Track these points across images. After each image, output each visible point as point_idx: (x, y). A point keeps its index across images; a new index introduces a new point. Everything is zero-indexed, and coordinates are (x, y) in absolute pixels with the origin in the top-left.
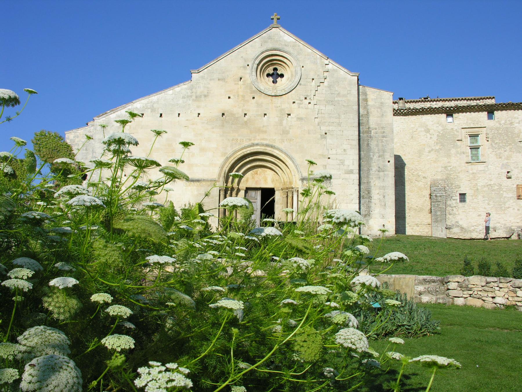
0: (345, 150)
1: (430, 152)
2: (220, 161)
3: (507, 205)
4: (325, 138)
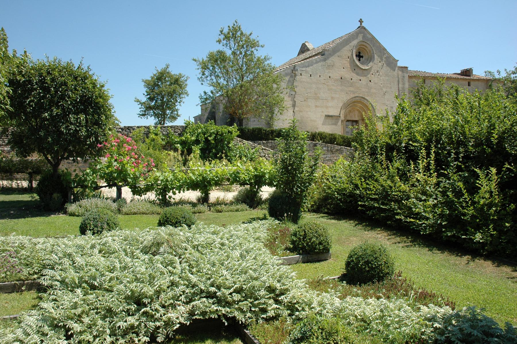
2: (341, 105)
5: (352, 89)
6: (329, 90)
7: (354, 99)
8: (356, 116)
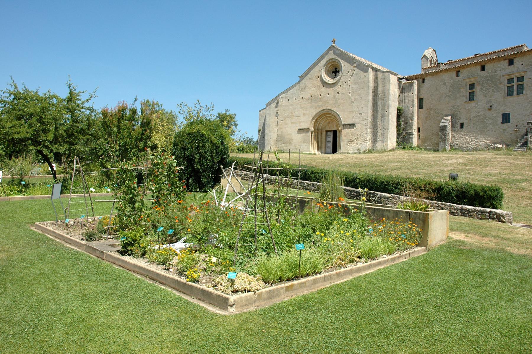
1: (445, 97)
2: (311, 118)
3: (488, 129)
5: (320, 103)
6: (302, 108)
7: (326, 111)
8: (335, 126)
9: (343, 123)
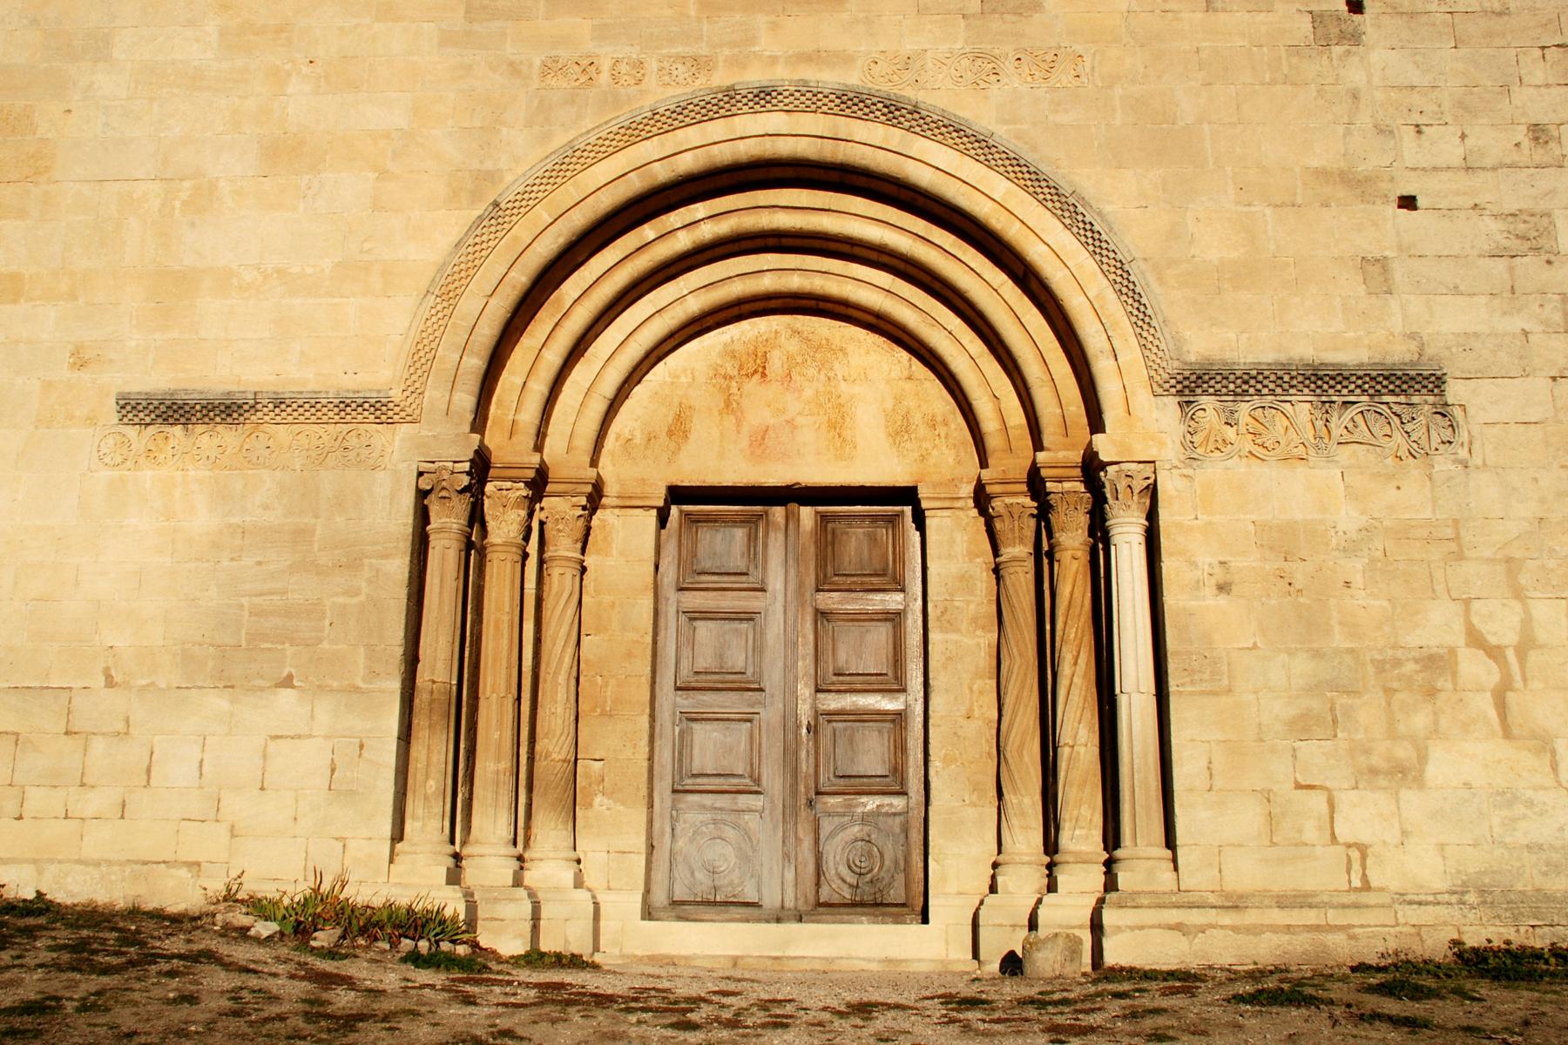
0: (1538, 133)
4: (1355, 38)
9: (1202, 342)
